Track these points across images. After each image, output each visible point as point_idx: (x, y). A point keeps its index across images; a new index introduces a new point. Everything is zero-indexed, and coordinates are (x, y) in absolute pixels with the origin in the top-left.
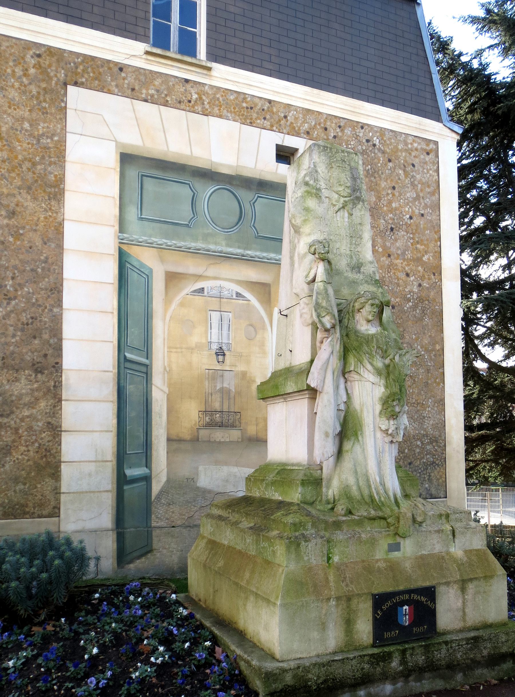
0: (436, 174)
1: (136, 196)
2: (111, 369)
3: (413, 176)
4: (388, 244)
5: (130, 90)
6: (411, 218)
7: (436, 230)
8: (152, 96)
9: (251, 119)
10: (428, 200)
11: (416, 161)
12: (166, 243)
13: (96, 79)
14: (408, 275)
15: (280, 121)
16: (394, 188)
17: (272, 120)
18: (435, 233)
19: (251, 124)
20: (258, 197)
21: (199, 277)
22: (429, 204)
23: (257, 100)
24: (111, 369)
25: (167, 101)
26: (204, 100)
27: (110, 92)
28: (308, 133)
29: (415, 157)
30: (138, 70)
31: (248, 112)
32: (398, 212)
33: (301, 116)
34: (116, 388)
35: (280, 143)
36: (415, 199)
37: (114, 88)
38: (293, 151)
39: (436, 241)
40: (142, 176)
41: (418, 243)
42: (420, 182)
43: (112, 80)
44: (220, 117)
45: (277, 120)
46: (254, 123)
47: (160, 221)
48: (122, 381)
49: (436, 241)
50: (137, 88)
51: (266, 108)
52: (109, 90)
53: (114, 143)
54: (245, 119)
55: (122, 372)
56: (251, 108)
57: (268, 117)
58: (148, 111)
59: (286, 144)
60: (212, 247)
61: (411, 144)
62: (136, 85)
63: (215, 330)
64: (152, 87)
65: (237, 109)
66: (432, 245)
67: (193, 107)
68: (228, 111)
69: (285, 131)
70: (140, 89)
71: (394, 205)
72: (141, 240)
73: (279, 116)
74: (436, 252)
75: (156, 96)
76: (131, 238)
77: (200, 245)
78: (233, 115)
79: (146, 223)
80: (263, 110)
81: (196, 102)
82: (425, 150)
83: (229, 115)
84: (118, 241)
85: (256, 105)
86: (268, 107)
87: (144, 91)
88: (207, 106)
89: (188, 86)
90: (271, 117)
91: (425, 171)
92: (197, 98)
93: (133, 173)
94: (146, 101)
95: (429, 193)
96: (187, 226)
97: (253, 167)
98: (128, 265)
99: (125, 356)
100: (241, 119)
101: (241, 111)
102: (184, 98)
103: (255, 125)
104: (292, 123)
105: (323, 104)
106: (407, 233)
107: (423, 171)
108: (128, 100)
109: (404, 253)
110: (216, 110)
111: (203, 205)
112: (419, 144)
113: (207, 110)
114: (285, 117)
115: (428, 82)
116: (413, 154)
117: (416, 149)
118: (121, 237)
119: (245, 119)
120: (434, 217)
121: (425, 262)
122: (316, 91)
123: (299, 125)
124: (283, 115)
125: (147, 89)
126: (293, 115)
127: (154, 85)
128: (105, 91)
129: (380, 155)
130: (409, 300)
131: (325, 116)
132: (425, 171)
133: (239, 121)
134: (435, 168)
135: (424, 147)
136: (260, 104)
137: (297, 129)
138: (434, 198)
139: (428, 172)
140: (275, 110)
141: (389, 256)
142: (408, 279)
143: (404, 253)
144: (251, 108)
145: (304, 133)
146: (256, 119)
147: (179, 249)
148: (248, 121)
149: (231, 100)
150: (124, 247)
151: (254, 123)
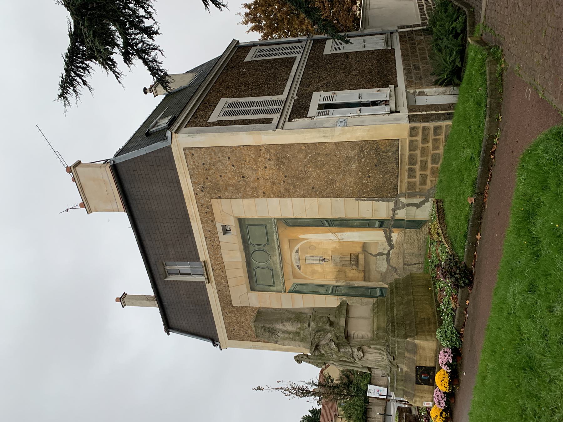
1: (266, 287)
3: (209, 164)
4: (252, 179)
6: (233, 166)
11: (201, 162)
14: (266, 168)
16: (221, 176)
21: (292, 266)
23: (208, 243)
30: (217, 285)
32: (233, 174)
36: (222, 163)
41: (245, 161)
44: (222, 257)
49: (241, 149)
58: (231, 283)
60: (278, 261)
63: (314, 262)
66: (245, 152)
71: (230, 176)
77: (278, 266)
85: (210, 244)
89: (215, 269)
93: (257, 288)
96: (272, 270)
106: (242, 168)
109: (254, 170)
111: (262, 265)
116: (197, 164)
117: (194, 162)
120: (227, 150)
121: (255, 156)
122: (190, 217)
129: (207, 184)
130: (280, 167)
138: (216, 151)
139: (203, 155)
141: (258, 179)
142: (268, 167)
143: (254, 170)
147: (283, 274)
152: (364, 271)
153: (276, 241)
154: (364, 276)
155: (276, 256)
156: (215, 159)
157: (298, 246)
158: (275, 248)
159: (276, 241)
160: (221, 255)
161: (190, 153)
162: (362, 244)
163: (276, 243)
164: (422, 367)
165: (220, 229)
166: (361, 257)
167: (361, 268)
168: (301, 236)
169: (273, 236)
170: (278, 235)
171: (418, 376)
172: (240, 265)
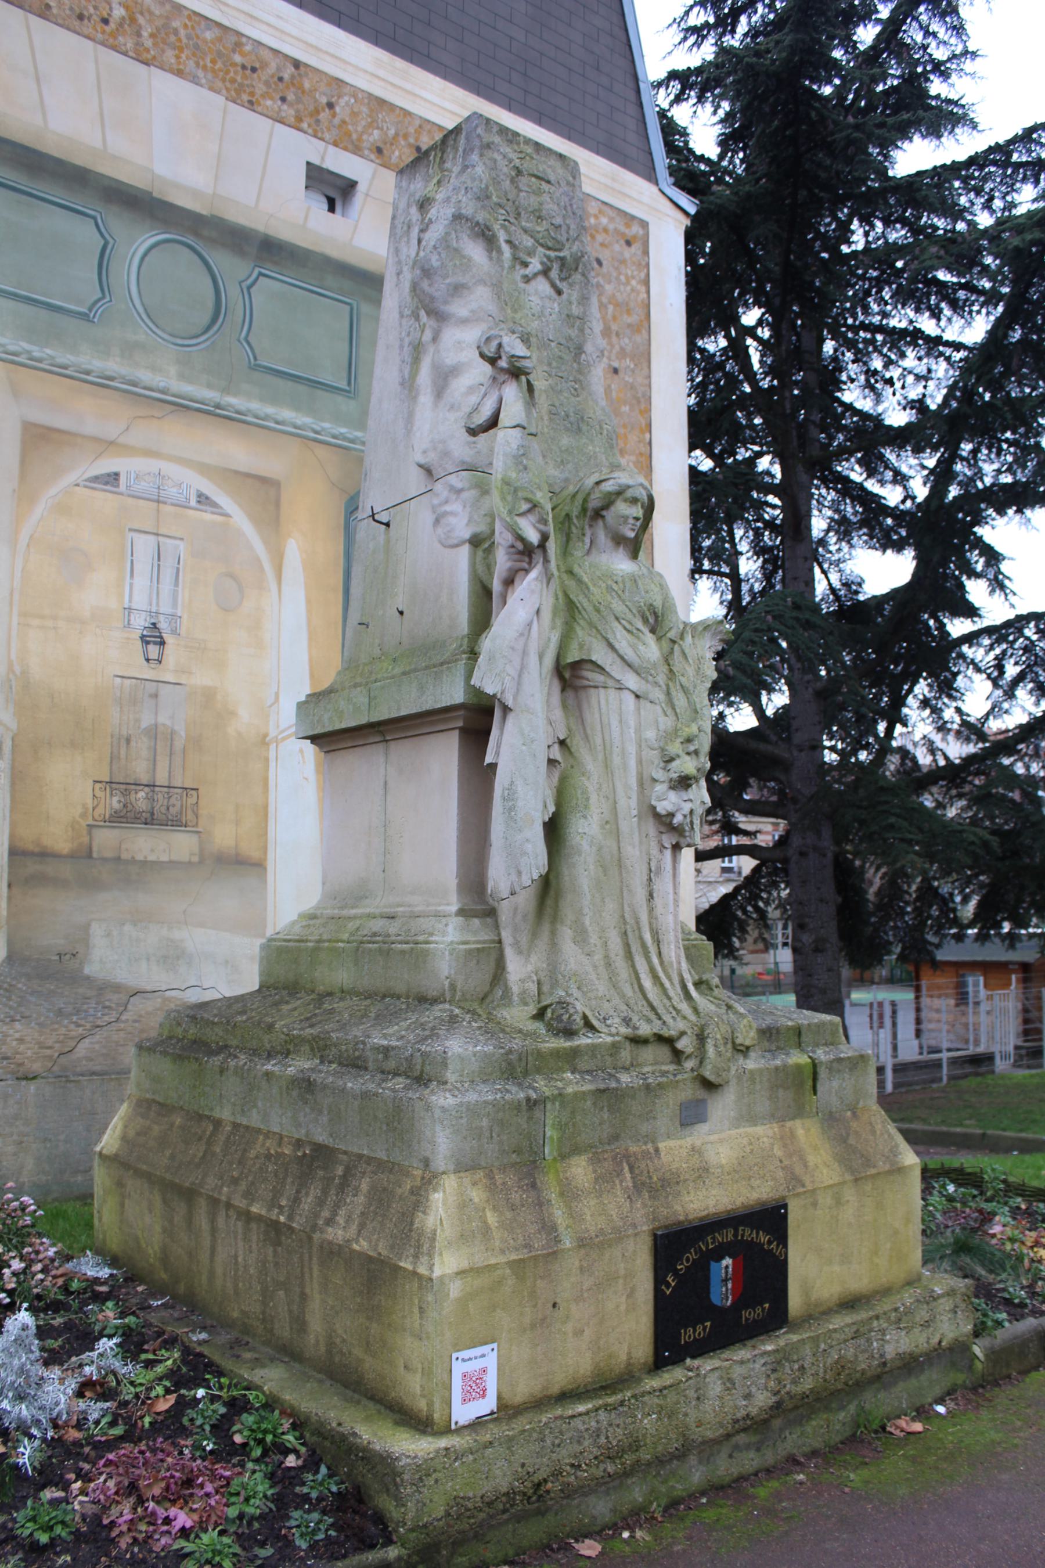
0: (643, 289)
7: (643, 406)
9: (252, 94)
10: (627, 340)
11: (605, 255)
12: (28, 352)
15: (317, 112)
17: (301, 107)
18: (642, 412)
19: (251, 105)
21: (108, 446)
22: (629, 349)
23: (266, 55)
26: (140, 27)
28: (379, 151)
29: (602, 245)
31: (245, 77)
33: (365, 109)
35: (316, 161)
38: (348, 187)
39: (642, 432)
42: (612, 300)
45: (311, 108)
46: (259, 104)
47: (15, 295)
49: (642, 432)
51: (286, 77)
54: (238, 92)
56: (254, 70)
57: (290, 97)
60: (145, 376)
61: (596, 217)
67: (114, 35)
69: (327, 136)
73: (316, 101)
74: (641, 454)
77: (113, 365)
78: (210, 76)
80: (281, 79)
82: (623, 234)
85: (265, 65)
86: (293, 77)
88: (149, 43)
90: (299, 101)
91: (622, 278)
95: (629, 326)
96: (84, 317)
100: (227, 89)
101: (227, 72)
103: (259, 109)
104: (344, 122)
105: (415, 95)
107: (618, 279)
111: (126, 270)
112: (611, 219)
114: (331, 106)
115: (632, 96)
119: (238, 92)
120: (640, 380)
122: (400, 63)
123: (359, 129)
124: (324, 100)
126: (347, 104)
131: (417, 122)
132: (622, 278)
133: (224, 92)
134: (643, 275)
135: (622, 228)
136: (273, 65)
137: (354, 136)
138: (638, 338)
139: (628, 283)
140: (307, 85)
144: (254, 70)
145: (371, 150)
146: (263, 96)
147: (60, 371)
148: (245, 97)
149: (205, 41)
151: (259, 104)
152: (85, 854)
153: (270, 410)
154: (44, 855)
155: (182, 377)
156: (614, 318)
157: (241, 520)
158: (226, 390)
159: (270, 410)
161: (635, 237)
162: (255, 855)
163: (255, 406)
164: (782, 1238)
165: (343, 163)
166: (180, 845)
167: (106, 839)
168: (293, 551)
170: (297, 434)
171: (729, 1235)
172: (120, 144)
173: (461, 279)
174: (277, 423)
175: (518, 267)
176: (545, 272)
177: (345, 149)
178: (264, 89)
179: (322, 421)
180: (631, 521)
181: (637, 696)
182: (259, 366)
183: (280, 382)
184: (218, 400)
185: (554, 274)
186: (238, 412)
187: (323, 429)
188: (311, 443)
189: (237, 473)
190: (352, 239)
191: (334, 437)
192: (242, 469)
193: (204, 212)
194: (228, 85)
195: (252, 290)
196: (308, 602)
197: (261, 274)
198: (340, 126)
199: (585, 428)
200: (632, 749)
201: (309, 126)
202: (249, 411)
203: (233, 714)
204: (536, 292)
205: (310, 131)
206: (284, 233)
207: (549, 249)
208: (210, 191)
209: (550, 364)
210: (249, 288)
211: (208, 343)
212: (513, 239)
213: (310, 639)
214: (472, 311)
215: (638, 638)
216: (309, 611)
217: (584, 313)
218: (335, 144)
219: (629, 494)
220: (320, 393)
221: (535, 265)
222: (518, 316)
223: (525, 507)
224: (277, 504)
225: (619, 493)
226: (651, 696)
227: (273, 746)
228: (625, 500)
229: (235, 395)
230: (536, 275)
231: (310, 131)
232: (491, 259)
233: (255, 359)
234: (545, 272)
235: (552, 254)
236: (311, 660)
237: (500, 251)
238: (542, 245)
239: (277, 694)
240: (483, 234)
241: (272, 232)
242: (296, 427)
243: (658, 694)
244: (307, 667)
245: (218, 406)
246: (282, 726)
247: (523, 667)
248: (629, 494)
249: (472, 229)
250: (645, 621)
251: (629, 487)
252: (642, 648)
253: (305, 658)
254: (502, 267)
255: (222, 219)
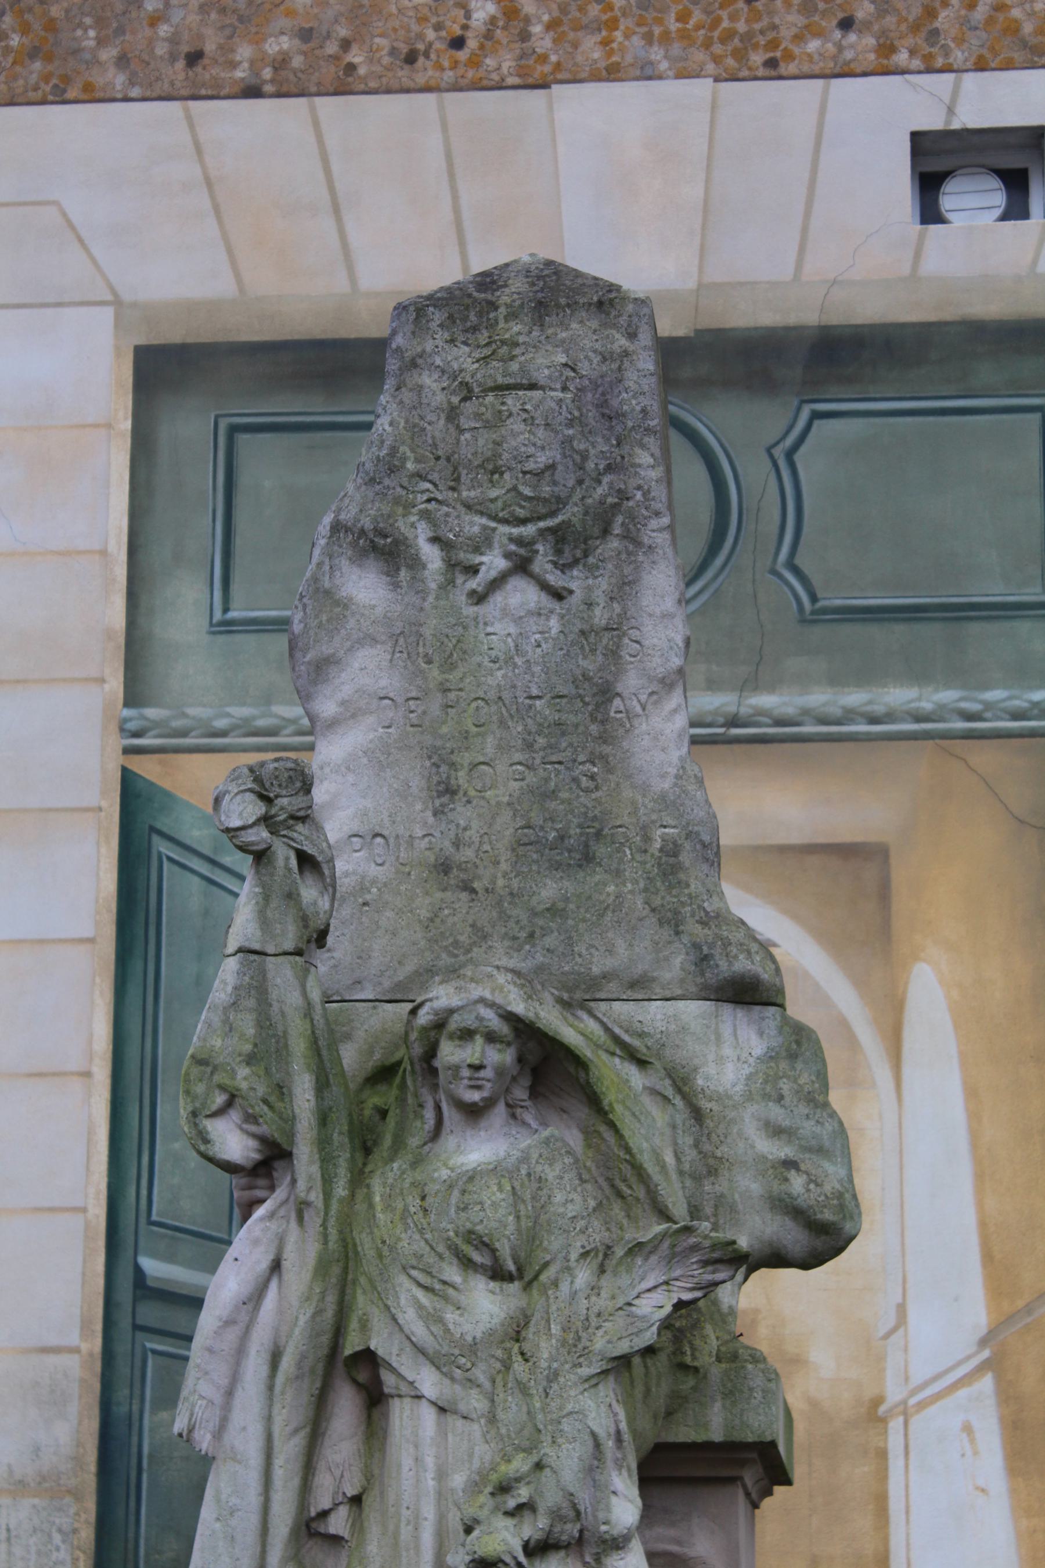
2: (74, 1338)
5: (181, 64)
8: (281, 63)
9: (773, 44)
13: (33, 53)
17: (890, 21)
20: (816, 415)
24: (74, 1338)
25: (351, 68)
27: (92, 95)
34: (93, 1425)
35: (933, 121)
37: (112, 71)
40: (234, 430)
43: (101, 42)
44: (612, 73)
46: (789, 56)
48: (122, 1393)
50: (210, 47)
52: (88, 87)
53: (109, 312)
54: (740, 55)
55: (122, 1348)
59: (972, 115)
62: (209, 32)
64: (283, 22)
65: (697, 16)
68: (649, 38)
69: (958, 56)
70: (227, 49)
72: (221, 724)
75: (297, 62)
76: (176, 724)
78: (676, 49)
79: (249, 642)
81: (489, 35)
83: (656, 53)
84: (117, 742)
87: (244, 52)
92: (493, 20)
94: (252, 92)
97: (787, 273)
98: (162, 847)
99: (139, 1271)
100: (717, 60)
101: (716, 22)
102: (431, 35)
103: (792, 68)
108: (174, 108)
110: (590, 49)
113: (543, 59)
118: (131, 726)
119: (740, 55)
125: (258, 40)
127: (290, 13)
128: (71, 94)
133: (710, 67)
146: (799, 38)
148: (757, 58)
150: (147, 768)
151: (789, 56)
153: (855, 698)
158: (752, 683)
159: (855, 698)
160: (647, 73)
163: (818, 698)
168: (928, 991)
169: (918, 674)
170: (926, 733)
173: (326, 650)
174: (874, 720)
175: (460, 579)
176: (521, 566)
177: (1008, 66)
178: (800, 21)
179: (986, 687)
180: (466, 1073)
181: (442, 1410)
182: (825, 611)
183: (875, 632)
184: (733, 709)
185: (542, 564)
186: (779, 722)
187: (988, 706)
188: (958, 746)
189: (783, 850)
190: (1035, 262)
191: (1017, 716)
192: (795, 839)
193: (681, 332)
194: (718, 49)
195: (798, 457)
196: (971, 1093)
197: (816, 415)
198: (990, 21)
199: (601, 850)
200: (429, 1511)
201: (912, 53)
202: (806, 712)
203: (798, 1361)
204: (505, 612)
205: (916, 63)
206: (870, 309)
207: (524, 522)
208: (691, 284)
209: (529, 746)
210: (790, 455)
211: (704, 597)
212: (440, 533)
213: (980, 1177)
214: (343, 703)
215: (446, 1298)
216: (974, 1117)
217: (624, 615)
218: (981, 66)
219: (455, 1023)
220: (975, 628)
221: (493, 562)
222: (454, 677)
223: (220, 1099)
224: (884, 894)
225: (439, 1025)
226: (462, 1407)
227: (896, 1425)
228: (451, 1037)
229: (771, 689)
230: (497, 583)
231: (916, 63)
232: (396, 586)
233: (814, 598)
234: (521, 566)
235: (529, 530)
236: (983, 1225)
237: (416, 564)
238: (505, 521)
239: (902, 1310)
240: (374, 547)
241: (835, 318)
242: (919, 718)
243: (475, 1402)
244: (974, 1240)
245: (734, 722)
246: (916, 1380)
247: (235, 1378)
248: (455, 1023)
249: (354, 544)
250: (467, 1264)
251: (451, 1011)
252: (450, 1316)
253: (970, 1219)
254: (423, 593)
255: (719, 333)
